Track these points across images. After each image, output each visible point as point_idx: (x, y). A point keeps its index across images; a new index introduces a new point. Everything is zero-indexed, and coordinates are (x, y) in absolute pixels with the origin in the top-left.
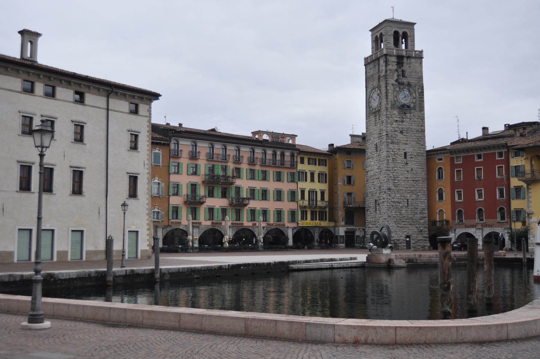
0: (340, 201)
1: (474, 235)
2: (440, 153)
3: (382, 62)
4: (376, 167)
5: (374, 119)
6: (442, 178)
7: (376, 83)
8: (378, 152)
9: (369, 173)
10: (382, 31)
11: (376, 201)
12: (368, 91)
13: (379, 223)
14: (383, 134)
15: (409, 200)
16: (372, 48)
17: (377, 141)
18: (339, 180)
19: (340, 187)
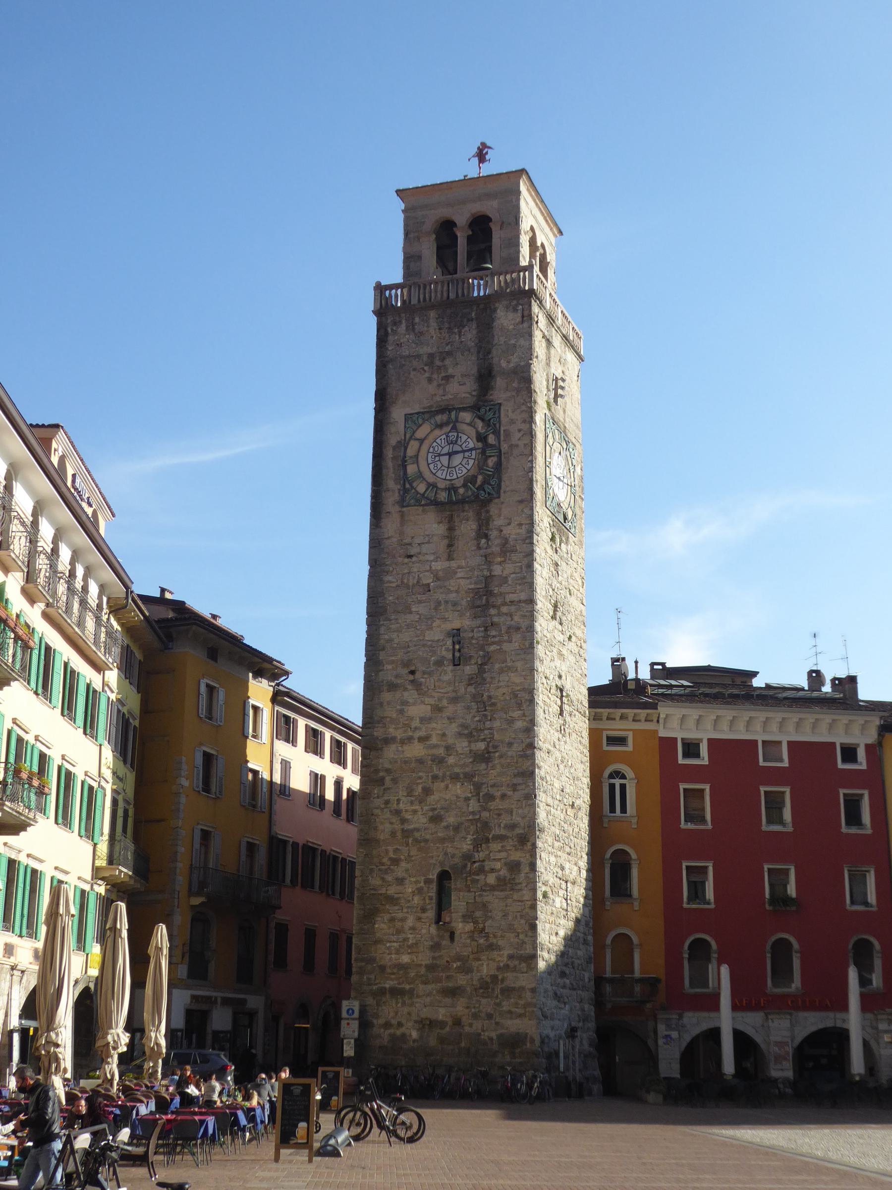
0: (180, 865)
1: (758, 1039)
2: (623, 717)
3: (505, 318)
4: (454, 728)
5: (439, 529)
6: (624, 810)
7: (462, 389)
8: (469, 669)
9: (390, 752)
10: (489, 207)
11: (444, 876)
12: (398, 414)
13: (476, 976)
14: (510, 597)
15: (569, 884)
16: (411, 259)
17: (465, 622)
18: (184, 767)
19: (183, 800)
